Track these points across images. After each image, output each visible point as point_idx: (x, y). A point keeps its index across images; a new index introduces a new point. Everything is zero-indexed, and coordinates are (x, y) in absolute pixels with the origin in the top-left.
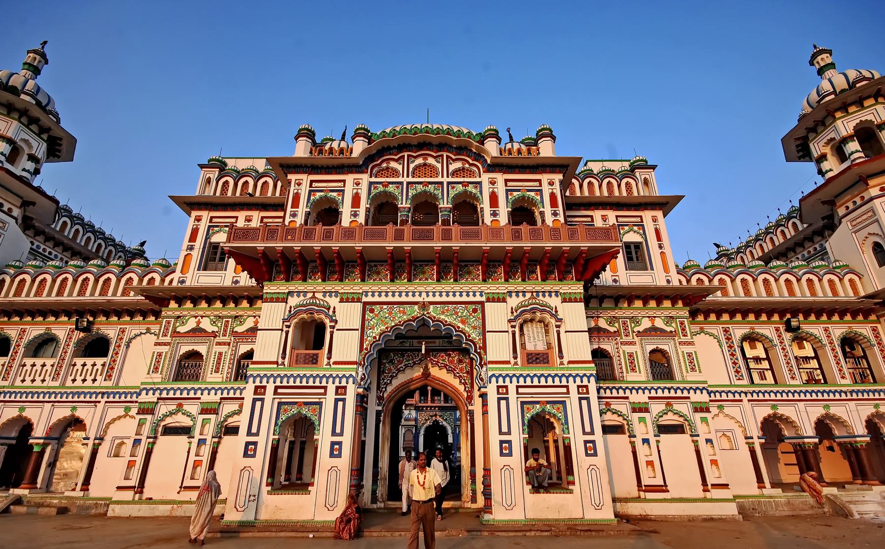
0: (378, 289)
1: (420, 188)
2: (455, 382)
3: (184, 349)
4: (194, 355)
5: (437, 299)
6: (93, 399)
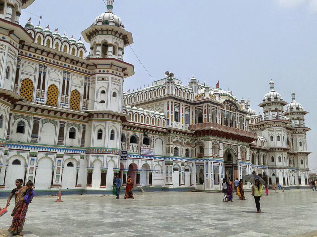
0: (226, 141)
3: (175, 146)
4: (176, 148)
5: (233, 144)
6: (151, 159)
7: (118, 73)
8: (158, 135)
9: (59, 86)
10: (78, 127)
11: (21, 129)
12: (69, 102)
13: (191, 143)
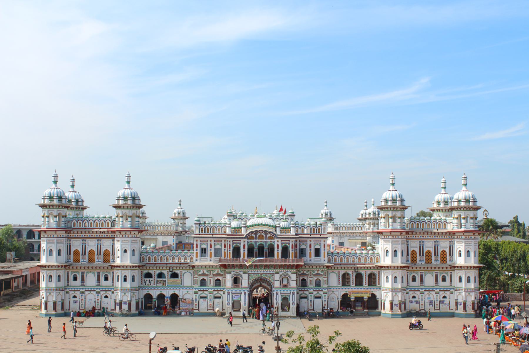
1: (260, 243)
2: (268, 287)
3: (201, 278)
4: (203, 280)
7: (127, 236)
8: (186, 269)
9: (95, 250)
10: (110, 273)
11: (75, 279)
12: (102, 258)
13: (222, 273)
